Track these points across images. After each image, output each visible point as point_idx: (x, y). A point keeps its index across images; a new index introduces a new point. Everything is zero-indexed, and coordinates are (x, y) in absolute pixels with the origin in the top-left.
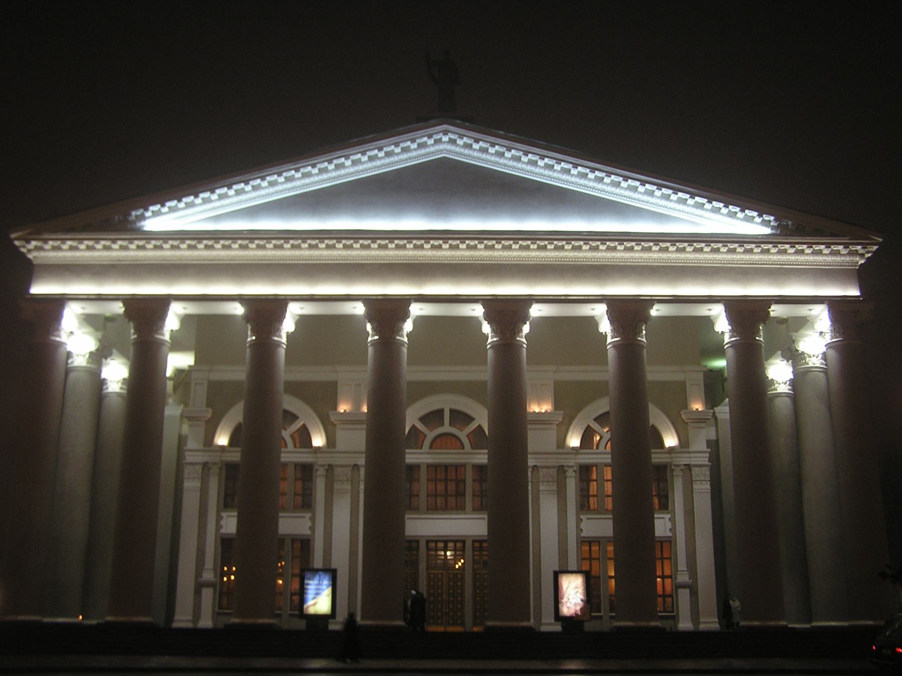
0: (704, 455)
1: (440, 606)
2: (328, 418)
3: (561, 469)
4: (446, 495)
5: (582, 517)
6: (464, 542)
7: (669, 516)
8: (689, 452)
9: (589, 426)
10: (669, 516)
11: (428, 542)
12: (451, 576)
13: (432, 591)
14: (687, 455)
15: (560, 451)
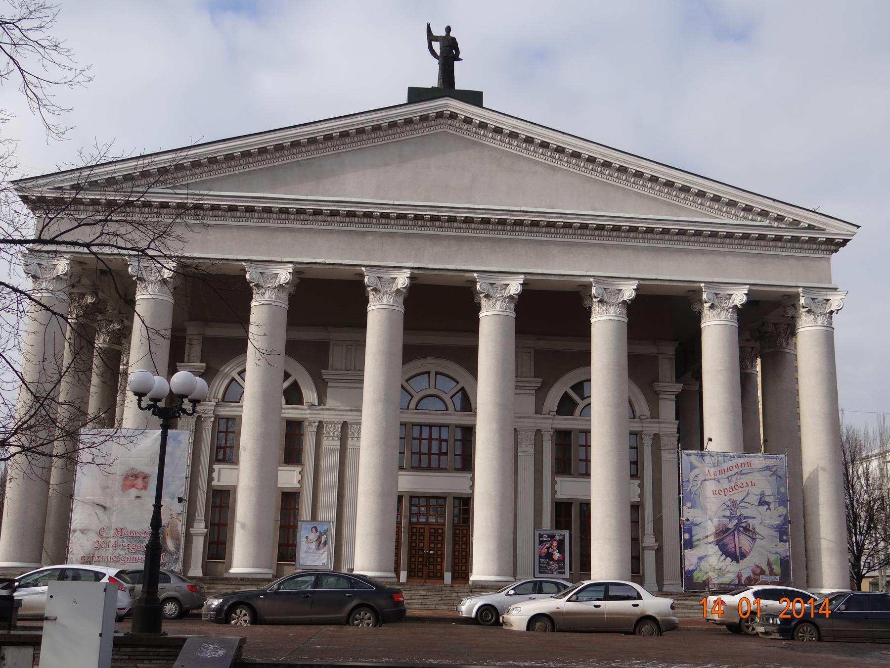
0: (672, 426)
1: (420, 560)
2: (321, 375)
3: (538, 432)
4: (430, 454)
5: (557, 479)
6: (445, 498)
7: (638, 482)
8: (659, 423)
9: (566, 394)
10: (638, 482)
11: (411, 497)
12: (432, 531)
13: (413, 552)
14: (657, 425)
15: (539, 415)
